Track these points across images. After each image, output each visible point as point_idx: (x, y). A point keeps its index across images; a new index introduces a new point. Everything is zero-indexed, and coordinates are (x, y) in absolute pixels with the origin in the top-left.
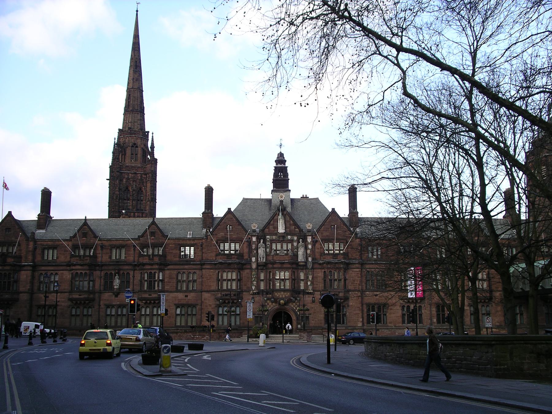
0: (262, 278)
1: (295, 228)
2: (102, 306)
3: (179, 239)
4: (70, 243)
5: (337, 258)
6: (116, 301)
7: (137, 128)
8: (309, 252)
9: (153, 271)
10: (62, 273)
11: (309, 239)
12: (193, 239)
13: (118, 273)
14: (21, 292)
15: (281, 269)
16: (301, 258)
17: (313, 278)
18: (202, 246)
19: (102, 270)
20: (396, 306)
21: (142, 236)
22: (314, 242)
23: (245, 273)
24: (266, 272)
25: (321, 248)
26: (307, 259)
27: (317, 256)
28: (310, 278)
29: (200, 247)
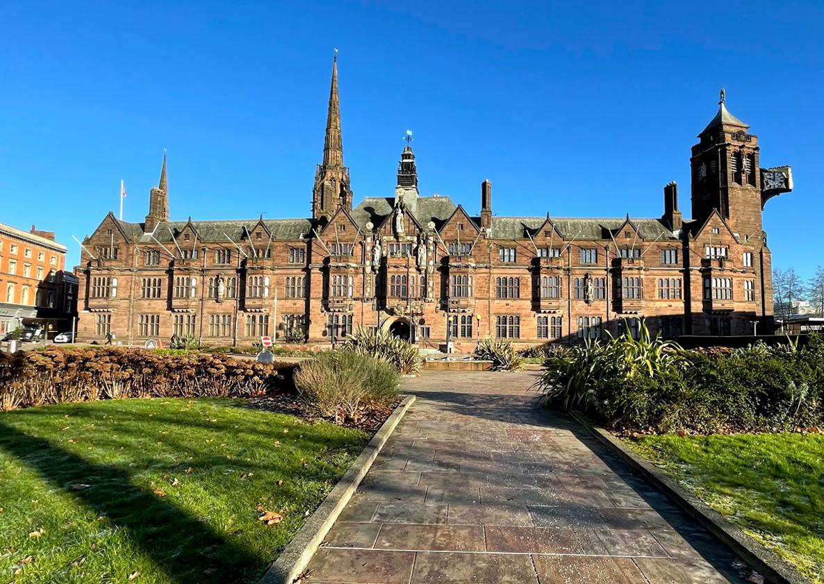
2: (205, 314)
8: (430, 254)
20: (530, 316)
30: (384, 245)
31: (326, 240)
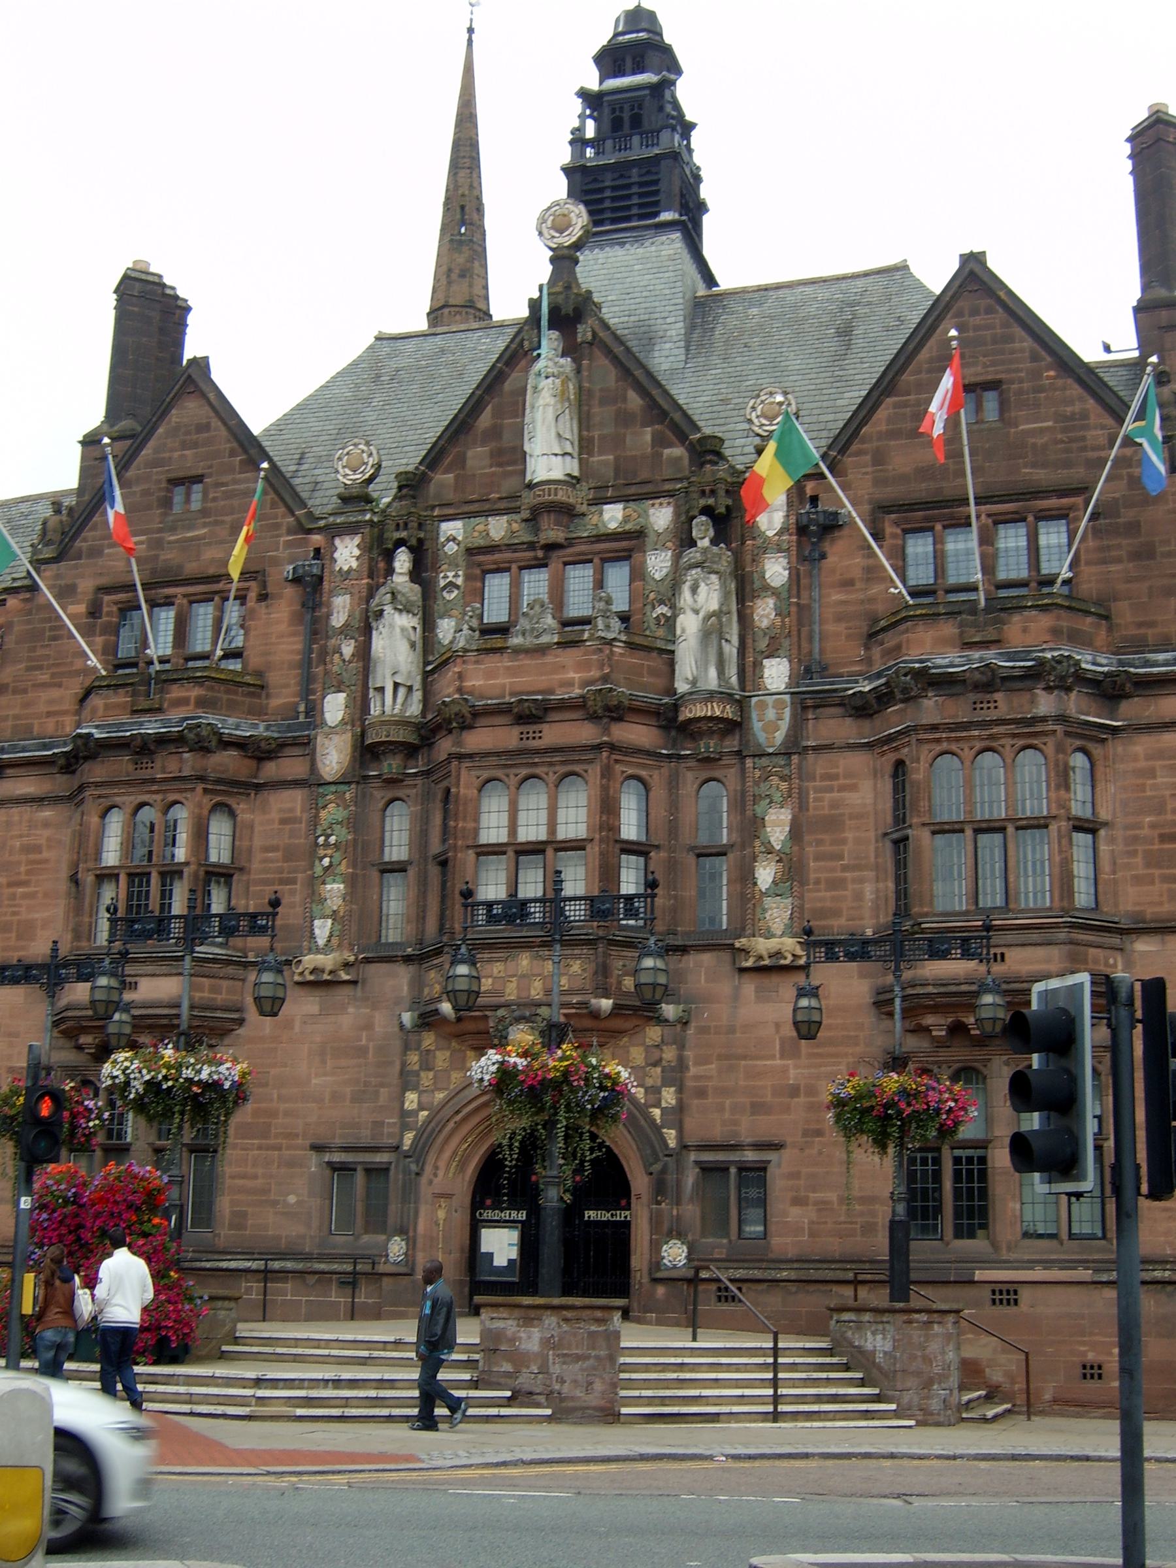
0: (397, 848)
1: (660, 441)
15: (524, 766)
16: (695, 668)
17: (796, 833)
24: (427, 797)
25: (873, 573)
26: (749, 672)
27: (840, 644)
28: (777, 826)
30: (451, 576)
31: (86, 585)
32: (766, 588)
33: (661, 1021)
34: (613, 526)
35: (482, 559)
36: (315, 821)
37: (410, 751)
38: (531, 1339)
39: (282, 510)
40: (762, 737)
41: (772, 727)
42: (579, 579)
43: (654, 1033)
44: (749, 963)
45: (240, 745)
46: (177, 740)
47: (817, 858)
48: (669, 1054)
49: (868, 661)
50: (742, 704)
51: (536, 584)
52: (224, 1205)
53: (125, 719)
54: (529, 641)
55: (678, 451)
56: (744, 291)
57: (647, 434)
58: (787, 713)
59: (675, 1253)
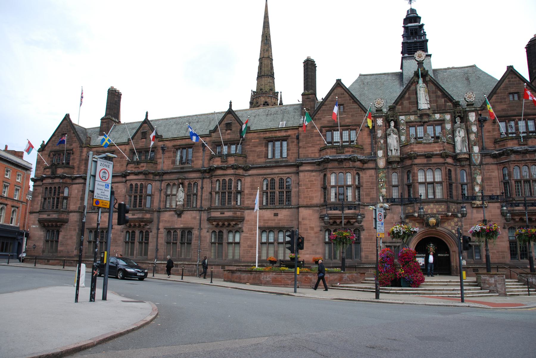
1: (445, 101)
2: (162, 230)
3: (265, 131)
4: (128, 148)
5: (526, 144)
6: (179, 223)
7: (267, 88)
8: (473, 137)
9: (227, 179)
10: (117, 187)
11: (472, 117)
12: (286, 129)
13: (182, 184)
14: (71, 212)
16: (460, 147)
17: (482, 180)
18: (298, 138)
19: (162, 180)
21: (215, 130)
22: (481, 122)
23: (367, 176)
24: (403, 172)
26: (470, 149)
27: (489, 144)
28: (479, 179)
29: (295, 140)
31: (319, 126)
32: (473, 132)
33: (457, 217)
34: (438, 118)
35: (409, 124)
36: (377, 177)
37: (398, 163)
38: (492, 280)
39: (363, 112)
40: (475, 162)
41: (476, 160)
42: (430, 129)
43: (456, 219)
44: (475, 206)
45: (361, 161)
46: (350, 159)
47: (487, 186)
48: (459, 224)
49: (495, 147)
50: (470, 155)
51: (420, 130)
52: (363, 254)
53: (335, 155)
54: (427, 142)
55: (450, 104)
56: (441, 69)
57: (443, 100)
58: (480, 157)
59: (464, 262)
